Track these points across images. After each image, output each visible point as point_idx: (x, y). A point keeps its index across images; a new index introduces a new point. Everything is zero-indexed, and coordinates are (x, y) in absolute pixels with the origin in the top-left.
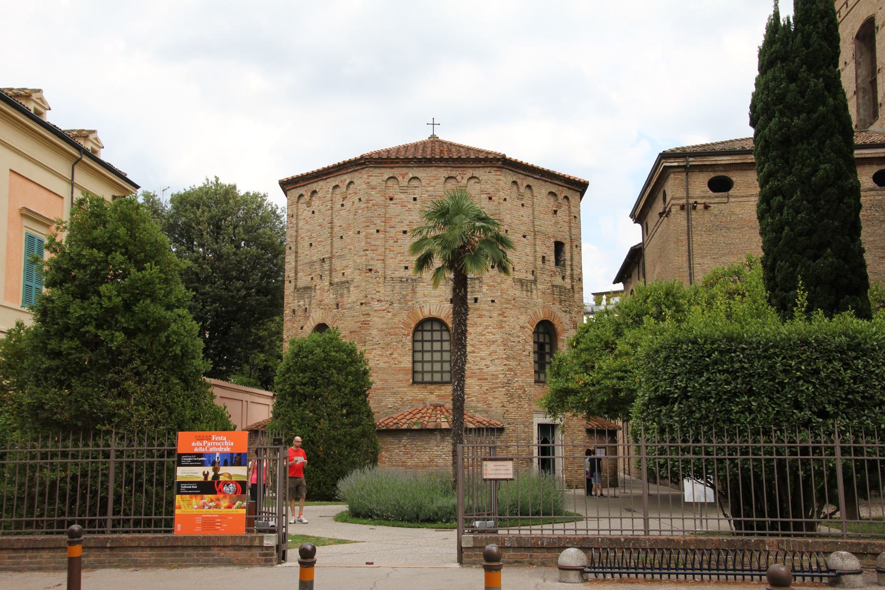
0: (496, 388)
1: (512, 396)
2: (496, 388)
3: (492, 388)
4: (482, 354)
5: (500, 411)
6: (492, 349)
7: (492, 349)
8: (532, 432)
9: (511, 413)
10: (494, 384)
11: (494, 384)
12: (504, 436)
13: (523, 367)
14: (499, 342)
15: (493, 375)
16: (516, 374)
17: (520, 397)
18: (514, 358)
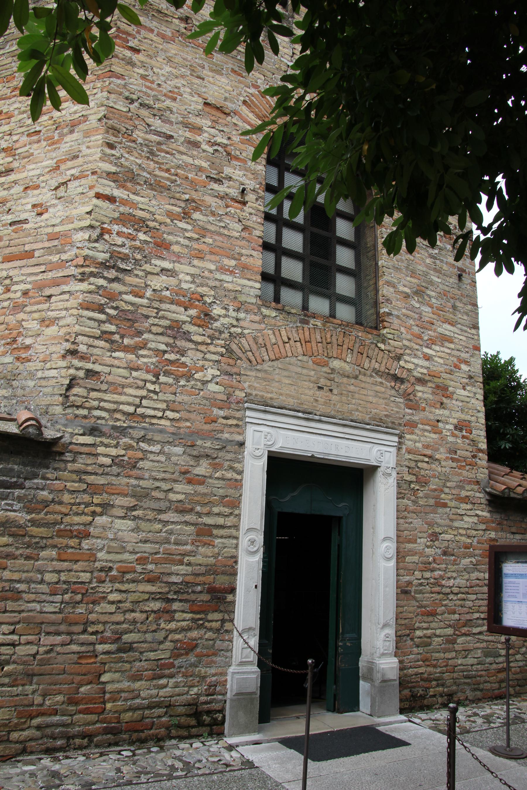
0: (55, 282)
1: (129, 320)
2: (55, 282)
3: (40, 287)
4: (32, 171)
5: (58, 372)
6: (65, 147)
7: (65, 147)
8: (237, 484)
9: (117, 388)
10: (52, 267)
11: (52, 267)
12: (51, 484)
13: (203, 232)
14: (93, 119)
15: (52, 237)
16: (162, 246)
17: (175, 330)
18: (157, 187)
